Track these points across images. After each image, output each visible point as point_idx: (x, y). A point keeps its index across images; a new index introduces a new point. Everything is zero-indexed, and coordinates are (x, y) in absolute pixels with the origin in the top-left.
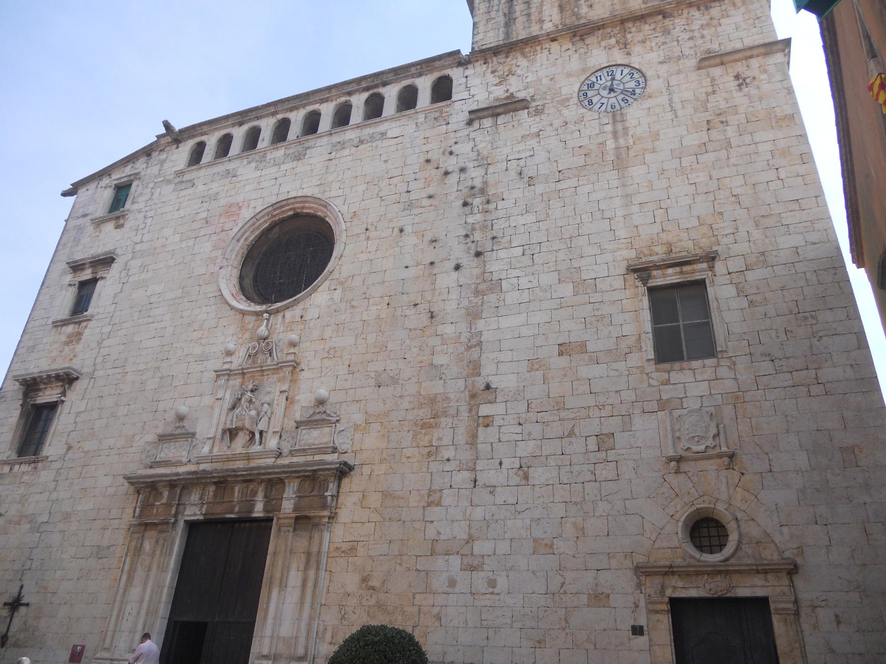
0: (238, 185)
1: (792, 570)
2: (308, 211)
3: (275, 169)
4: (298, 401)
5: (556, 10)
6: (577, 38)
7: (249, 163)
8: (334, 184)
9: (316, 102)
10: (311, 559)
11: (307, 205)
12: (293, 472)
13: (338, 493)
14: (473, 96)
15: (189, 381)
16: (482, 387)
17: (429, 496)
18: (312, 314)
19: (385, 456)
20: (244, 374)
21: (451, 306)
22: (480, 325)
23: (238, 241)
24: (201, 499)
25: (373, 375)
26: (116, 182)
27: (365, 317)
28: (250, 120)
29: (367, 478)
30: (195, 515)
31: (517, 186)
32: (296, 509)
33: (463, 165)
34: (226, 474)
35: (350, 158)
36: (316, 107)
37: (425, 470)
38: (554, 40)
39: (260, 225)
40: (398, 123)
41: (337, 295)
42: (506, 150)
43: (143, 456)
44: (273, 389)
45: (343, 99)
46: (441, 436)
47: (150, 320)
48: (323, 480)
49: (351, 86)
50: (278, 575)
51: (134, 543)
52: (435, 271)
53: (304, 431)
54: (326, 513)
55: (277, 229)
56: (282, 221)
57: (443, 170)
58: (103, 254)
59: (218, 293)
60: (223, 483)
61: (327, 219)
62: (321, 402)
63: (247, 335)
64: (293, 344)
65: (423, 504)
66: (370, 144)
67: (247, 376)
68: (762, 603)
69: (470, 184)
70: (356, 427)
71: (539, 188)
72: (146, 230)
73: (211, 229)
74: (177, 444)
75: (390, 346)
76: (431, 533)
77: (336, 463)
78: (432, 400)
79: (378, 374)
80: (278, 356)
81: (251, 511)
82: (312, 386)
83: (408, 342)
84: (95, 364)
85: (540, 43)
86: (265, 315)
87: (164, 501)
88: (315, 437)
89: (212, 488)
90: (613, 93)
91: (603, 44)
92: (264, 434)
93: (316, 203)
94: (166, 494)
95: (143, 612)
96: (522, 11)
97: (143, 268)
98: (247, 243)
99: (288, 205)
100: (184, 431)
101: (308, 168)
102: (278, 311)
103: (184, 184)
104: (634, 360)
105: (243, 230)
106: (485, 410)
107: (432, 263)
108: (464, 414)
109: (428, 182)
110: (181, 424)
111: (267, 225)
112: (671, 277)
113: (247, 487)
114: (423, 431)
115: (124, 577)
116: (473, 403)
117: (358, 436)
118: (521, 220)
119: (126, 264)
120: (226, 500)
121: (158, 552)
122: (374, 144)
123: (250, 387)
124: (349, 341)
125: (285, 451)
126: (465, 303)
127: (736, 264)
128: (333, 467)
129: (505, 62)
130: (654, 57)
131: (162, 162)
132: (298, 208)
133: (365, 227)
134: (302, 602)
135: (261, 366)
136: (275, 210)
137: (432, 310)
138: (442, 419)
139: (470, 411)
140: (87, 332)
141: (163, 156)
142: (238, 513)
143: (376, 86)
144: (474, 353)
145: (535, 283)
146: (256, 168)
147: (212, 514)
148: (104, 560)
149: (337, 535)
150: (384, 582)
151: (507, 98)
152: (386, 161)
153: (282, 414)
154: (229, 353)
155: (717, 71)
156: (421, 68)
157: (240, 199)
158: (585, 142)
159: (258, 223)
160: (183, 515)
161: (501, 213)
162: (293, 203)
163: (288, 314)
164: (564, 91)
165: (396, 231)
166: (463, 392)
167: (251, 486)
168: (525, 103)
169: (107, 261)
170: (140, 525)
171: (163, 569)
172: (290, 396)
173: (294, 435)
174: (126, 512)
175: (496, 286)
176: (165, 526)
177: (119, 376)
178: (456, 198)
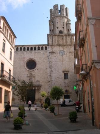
1: (71, 93)
12: (37, 86)
21: (49, 73)
48: (39, 87)
68: (69, 95)
82: (37, 78)
88: (38, 83)
90: (62, 54)
104: (63, 79)
112: (66, 73)
124: (40, 75)
127: (70, 72)
130: (66, 50)
135: (31, 76)
154: (27, 74)
155: (70, 53)
157: (25, 57)
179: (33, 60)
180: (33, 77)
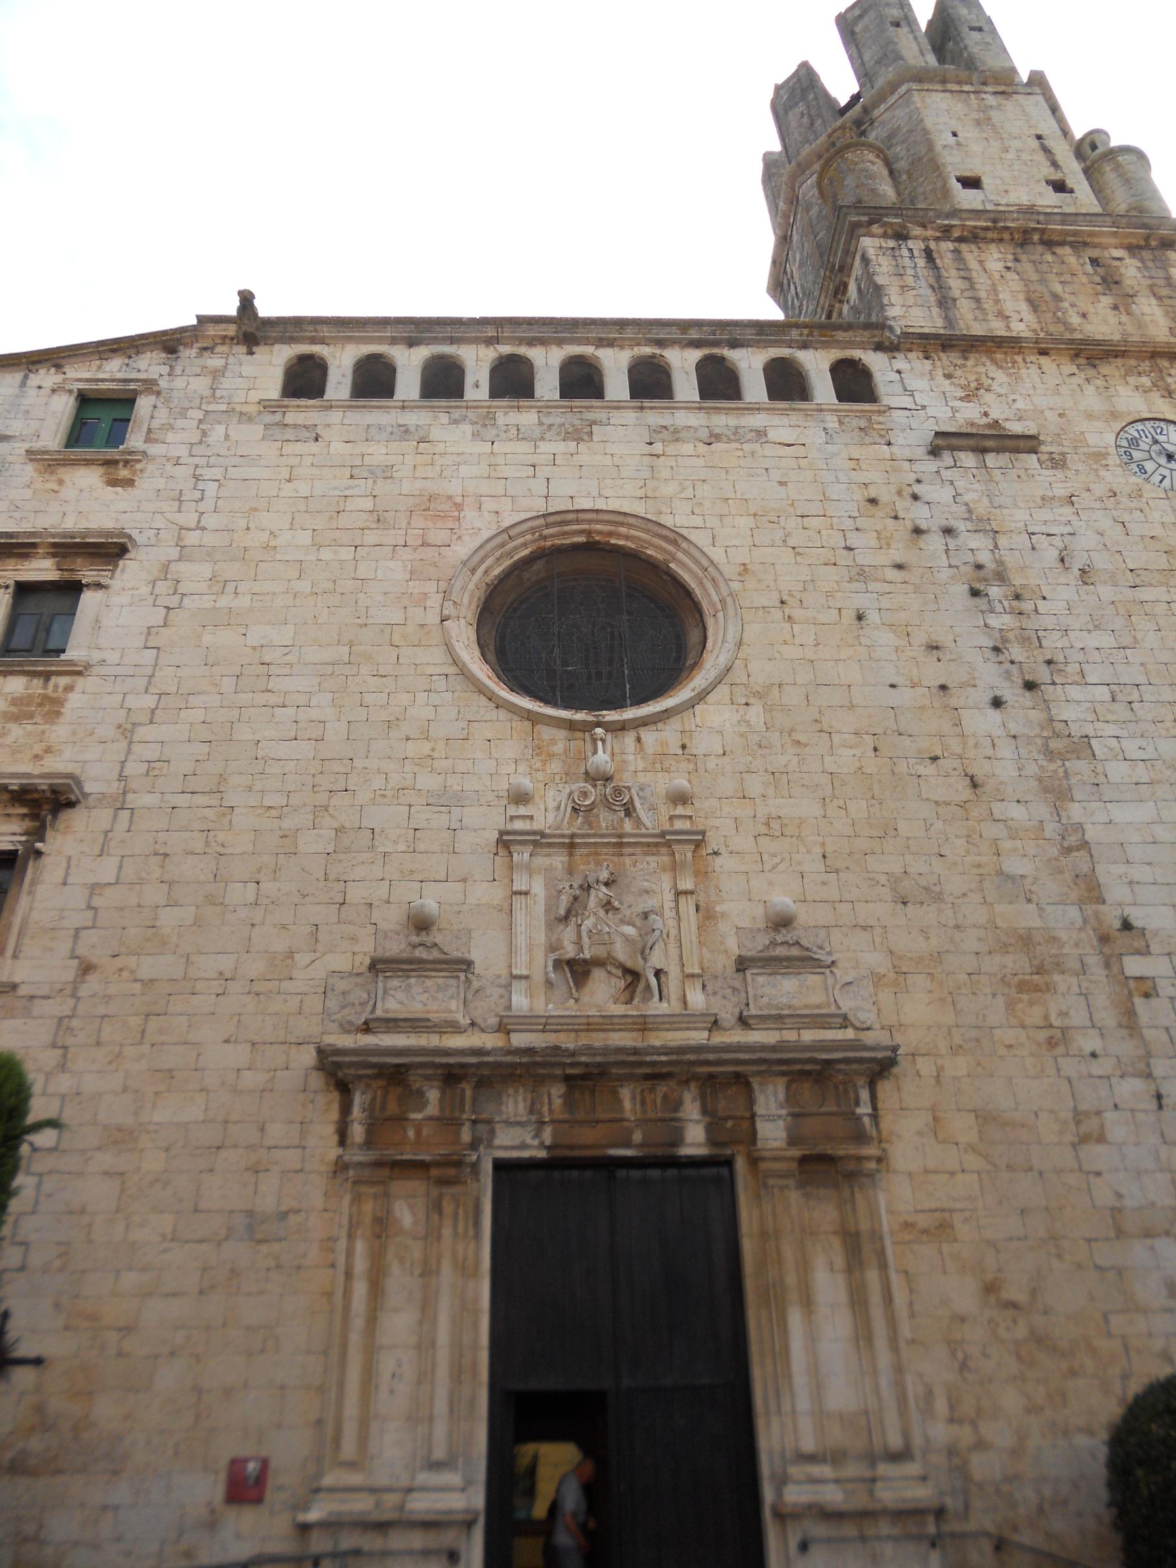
0: (439, 461)
2: (621, 542)
3: (524, 447)
4: (723, 915)
5: (1024, 307)
6: (1082, 361)
7: (456, 422)
8: (676, 503)
9: (587, 342)
10: (858, 1248)
11: (623, 530)
13: (875, 1108)
14: (924, 407)
15: (421, 846)
16: (1117, 924)
17: (1078, 1123)
18: (702, 744)
19: (957, 1040)
20: (572, 846)
22: (1075, 812)
23: (473, 571)
24: (531, 1111)
25: (883, 879)
26: (82, 386)
27: (831, 767)
28: (435, 341)
29: (933, 1081)
30: (523, 1146)
31: (1062, 580)
32: (792, 1141)
33: (944, 523)
34: (612, 1059)
35: (700, 462)
36: (588, 350)
37: (1053, 1072)
38: (1043, 353)
39: (516, 549)
40: (785, 421)
41: (756, 714)
42: (1021, 515)
43: (333, 1004)
44: (651, 884)
45: (647, 350)
46: (1064, 1008)
47: (273, 699)
49: (667, 329)
50: (791, 1279)
51: (368, 1207)
52: (954, 702)
53: (761, 979)
54: (871, 1150)
55: (539, 565)
56: (558, 551)
57: (909, 525)
58: (100, 533)
59: (452, 670)
60: (586, 1078)
61: (672, 565)
62: (782, 922)
63: (555, 766)
64: (680, 798)
65: (1069, 1138)
66: (737, 445)
67: (579, 851)
69: (969, 558)
70: (877, 979)
71: (1106, 592)
72: (207, 505)
73: (390, 538)
74: (429, 983)
75: (903, 827)
76: (1103, 1196)
77: (886, 1048)
78: (1026, 940)
79: (894, 881)
80: (651, 820)
81: (677, 1139)
83: (939, 825)
84: (121, 777)
85: (1020, 351)
86: (599, 730)
87: (432, 1109)
89: (557, 1091)
91: (1132, 380)
92: (663, 979)
93: (648, 531)
94: (433, 1095)
95: (443, 1372)
96: (962, 291)
97: (218, 584)
98: (488, 579)
99: (578, 521)
100: (435, 954)
101: (608, 460)
102: (621, 727)
103: (288, 430)
105: (482, 553)
106: (1134, 966)
107: (943, 687)
108: (1098, 972)
109: (884, 542)
110: (424, 937)
111: (526, 552)
113: (652, 1090)
114: (1025, 997)
115: (360, 1289)
116: (1107, 950)
117: (885, 997)
118: (1092, 641)
119: (166, 567)
120: (600, 1115)
121: (447, 1232)
122: (747, 447)
123: (604, 875)
124: (806, 808)
125: (728, 1014)
126: (1032, 769)
128: (880, 1055)
129: (964, 366)
131: (217, 375)
132: (600, 533)
133: (775, 597)
134: (863, 1336)
136: (547, 526)
137: (970, 772)
138: (1057, 978)
139: (1107, 966)
140: (74, 701)
141: (215, 362)
142: (640, 1146)
143: (716, 343)
144: (1080, 861)
145: (1150, 753)
146: (476, 435)
147: (571, 1147)
148: (276, 1247)
149: (896, 1199)
150: (1033, 1293)
151: (989, 426)
152: (781, 483)
153: (694, 939)
154: (520, 798)
156: (811, 334)
157: (454, 488)
158: (1158, 531)
159: (512, 545)
160: (490, 1145)
161: (1049, 622)
162: (590, 521)
163: (649, 736)
164: (1092, 439)
165: (849, 617)
166: (1080, 929)
167: (662, 1089)
168: (1035, 443)
169: (110, 551)
170: (378, 1164)
171: (466, 1270)
172: (702, 904)
173: (737, 984)
174: (315, 1134)
175: (1083, 746)
176: (451, 1172)
177: (210, 813)
178: (952, 577)
179: (632, 557)
180: (663, 842)
